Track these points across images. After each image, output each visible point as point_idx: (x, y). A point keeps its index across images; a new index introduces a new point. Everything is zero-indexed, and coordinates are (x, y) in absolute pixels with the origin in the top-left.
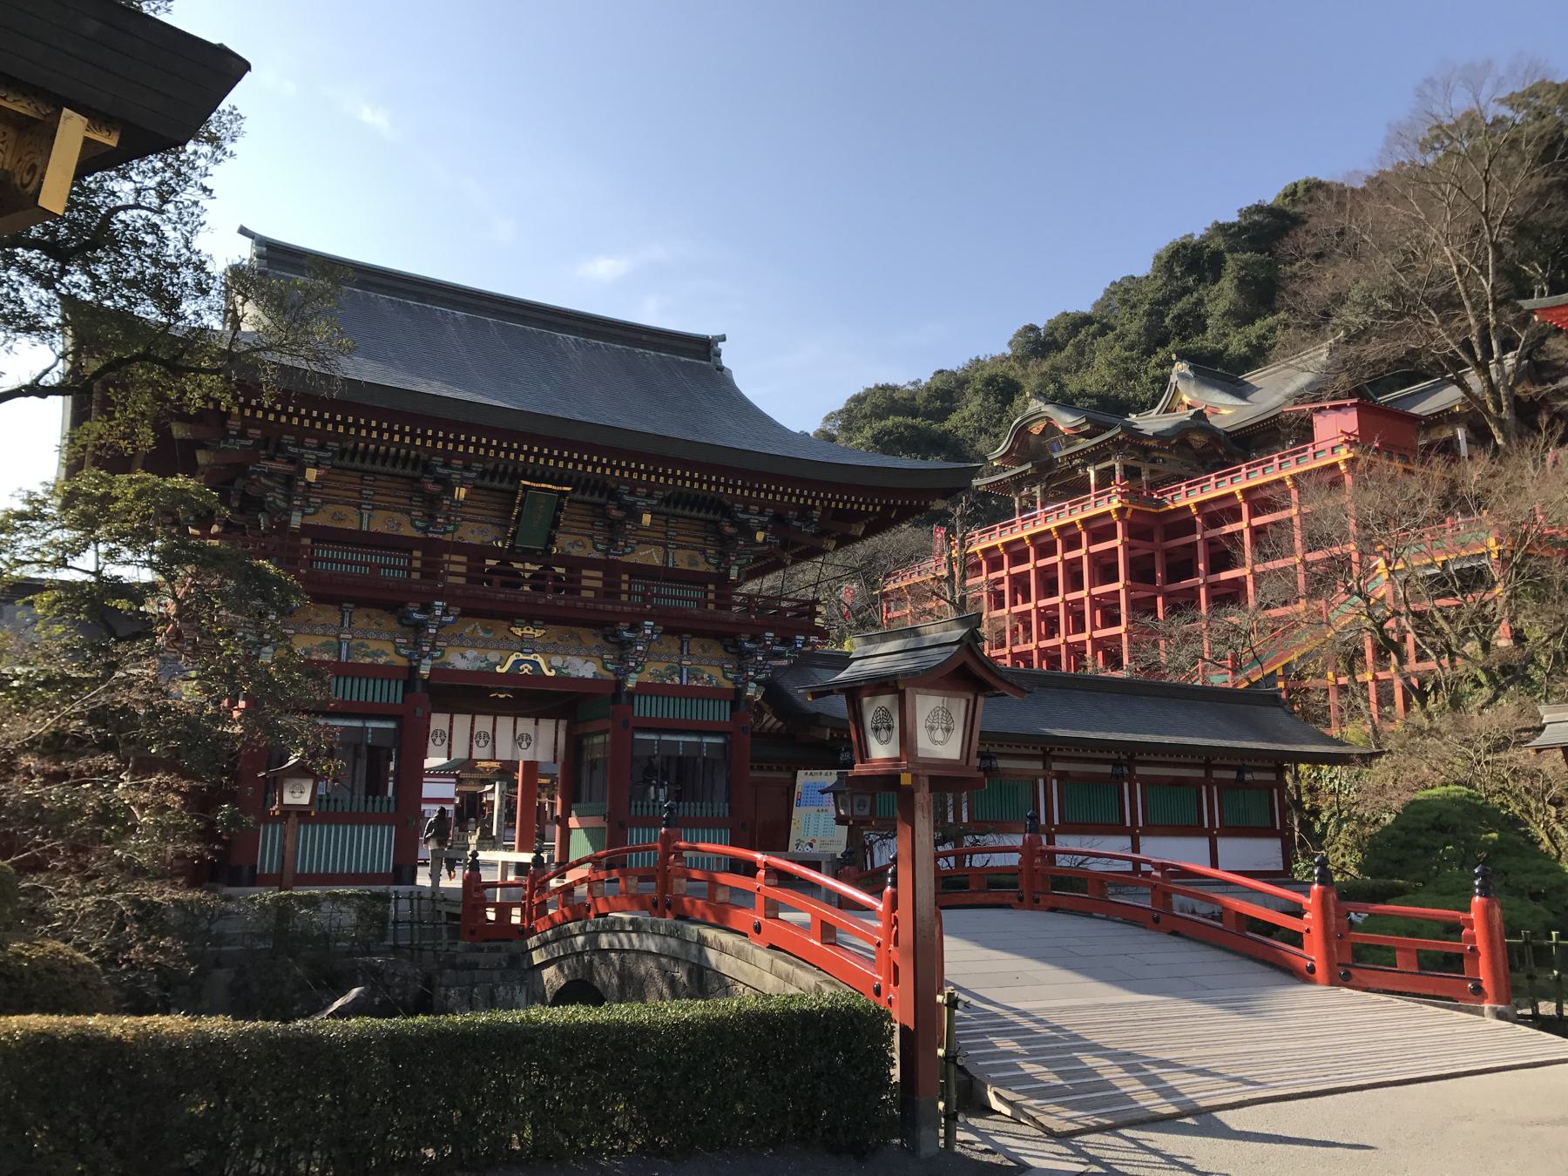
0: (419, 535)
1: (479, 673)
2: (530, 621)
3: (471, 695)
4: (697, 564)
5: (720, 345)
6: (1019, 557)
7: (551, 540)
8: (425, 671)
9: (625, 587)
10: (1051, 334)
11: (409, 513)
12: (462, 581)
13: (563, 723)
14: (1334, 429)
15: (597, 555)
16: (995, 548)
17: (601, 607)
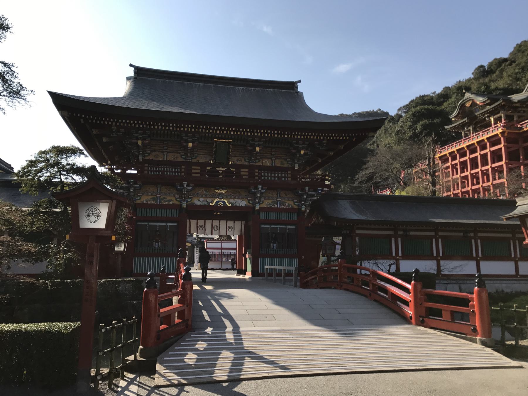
0: (184, 160)
1: (204, 206)
2: (221, 188)
3: (207, 213)
5: (298, 84)
6: (463, 155)
7: (228, 160)
8: (184, 206)
9: (257, 174)
11: (179, 153)
12: (247, 177)
13: (243, 222)
15: (246, 163)
16: (454, 152)
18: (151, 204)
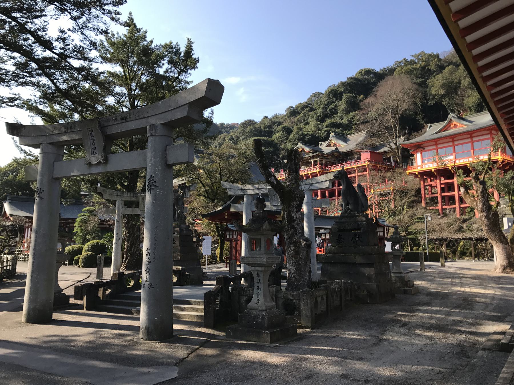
10: (297, 109)
14: (366, 156)
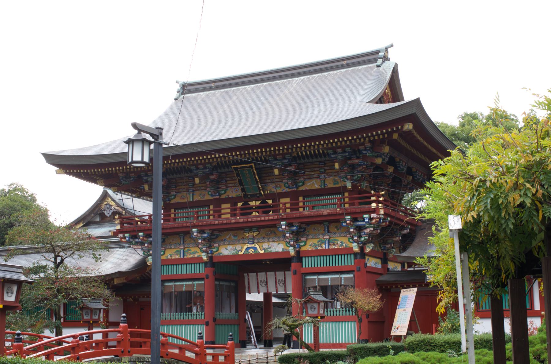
1: (233, 256)
4: (338, 183)
15: (287, 190)
17: (263, 218)
18: (175, 259)
